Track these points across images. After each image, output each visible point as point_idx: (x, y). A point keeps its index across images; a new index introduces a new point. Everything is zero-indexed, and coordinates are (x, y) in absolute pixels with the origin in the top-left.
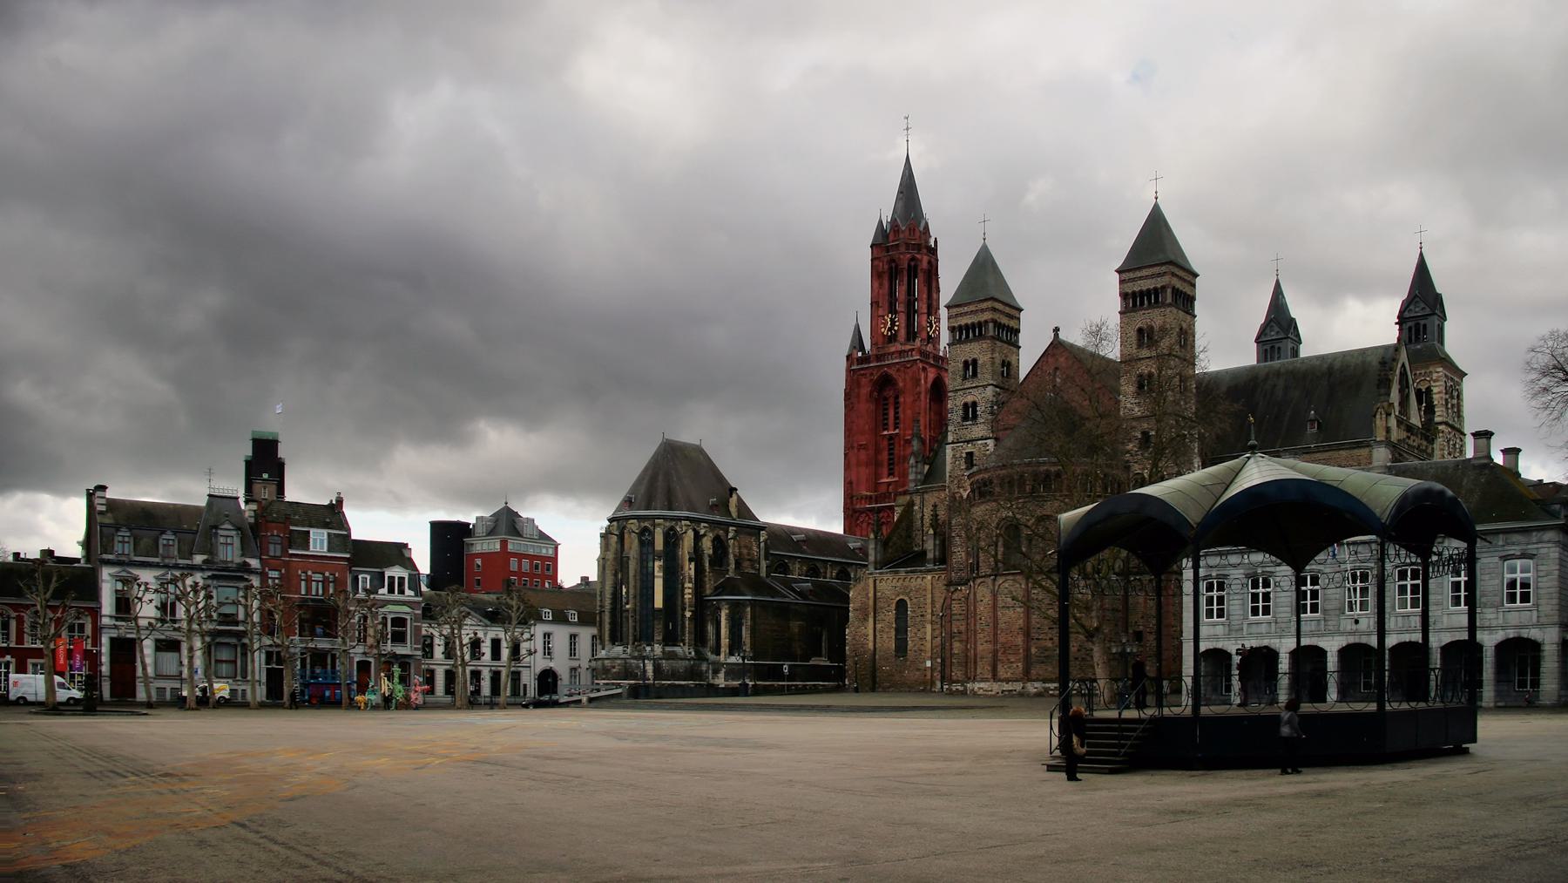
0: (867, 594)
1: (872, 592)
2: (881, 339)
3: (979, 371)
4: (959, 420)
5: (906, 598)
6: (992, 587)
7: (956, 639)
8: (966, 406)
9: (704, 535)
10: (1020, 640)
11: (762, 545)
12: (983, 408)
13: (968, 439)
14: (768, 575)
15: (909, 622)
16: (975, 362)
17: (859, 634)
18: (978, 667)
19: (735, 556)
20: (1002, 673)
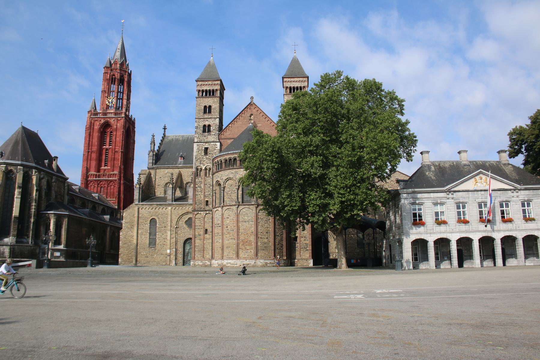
0: (134, 215)
1: (137, 214)
2: (105, 106)
3: (212, 111)
4: (201, 132)
5: (156, 218)
6: (236, 211)
7: (197, 238)
8: (205, 126)
9: (43, 178)
10: (252, 238)
11: (66, 188)
12: (214, 128)
13: (205, 141)
14: (68, 204)
15: (157, 230)
16: (210, 107)
17: (128, 235)
18: (225, 252)
19: (55, 192)
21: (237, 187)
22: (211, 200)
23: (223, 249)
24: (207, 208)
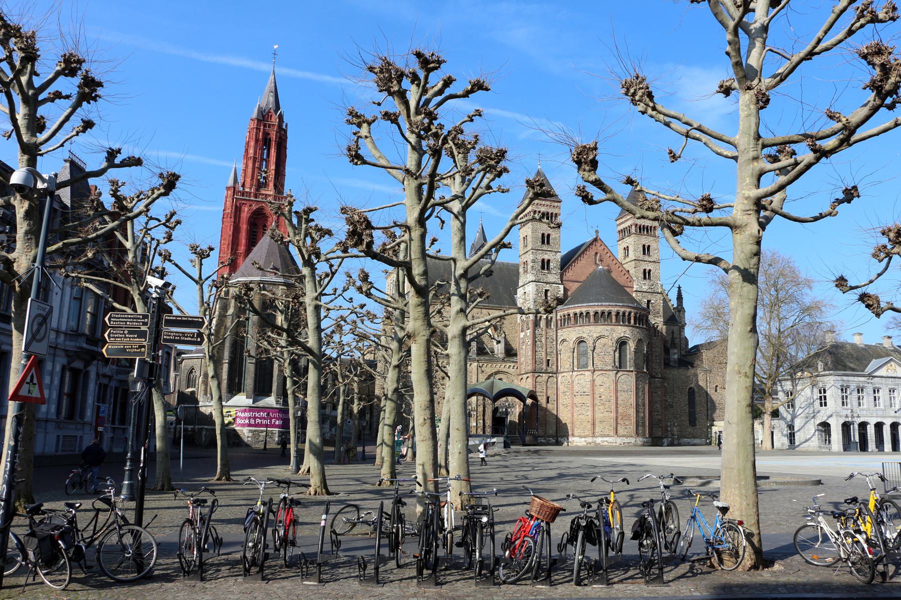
4: (539, 268)
6: (614, 378)
8: (543, 260)
18: (597, 428)
20: (621, 431)
21: (614, 348)
22: (555, 359)
23: (594, 424)
24: (549, 370)
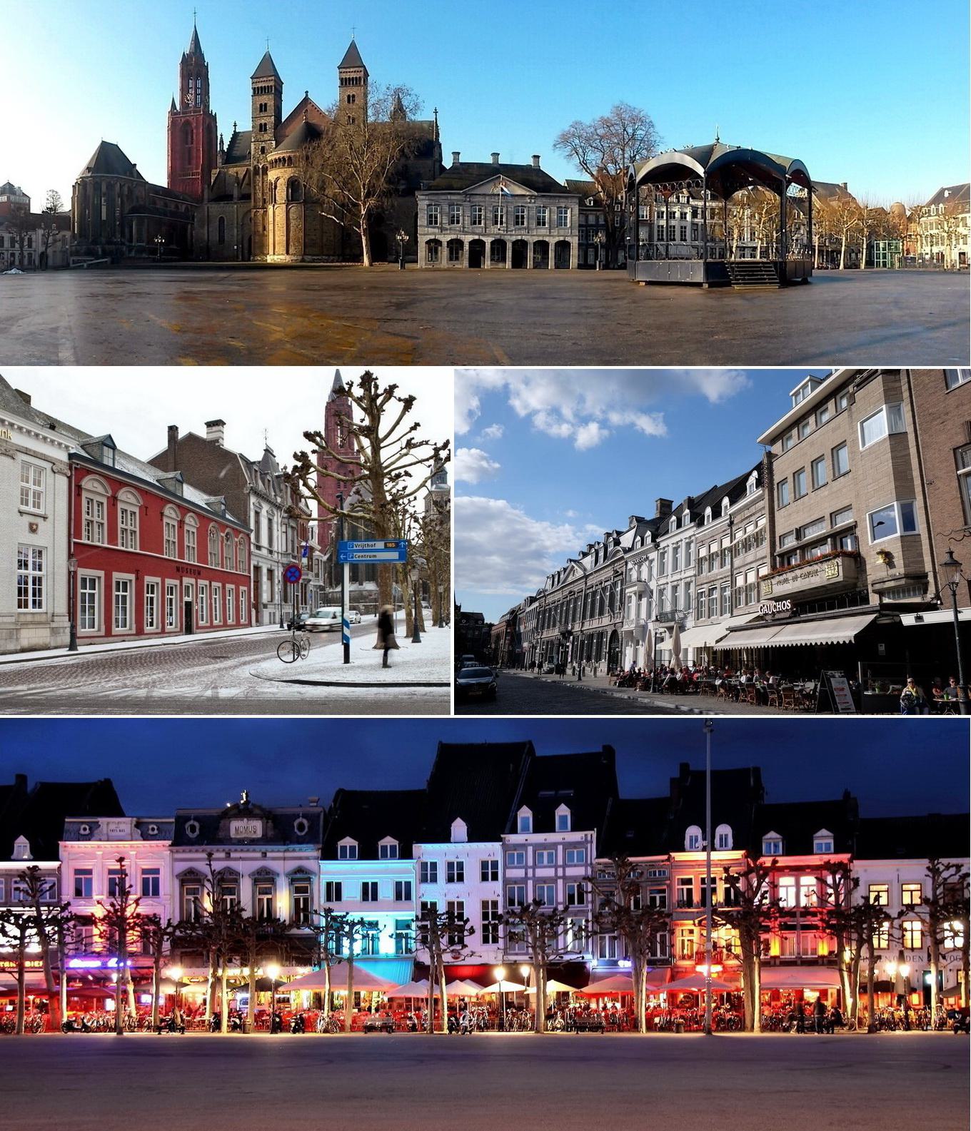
8: (261, 124)
16: (266, 104)
20: (291, 251)
